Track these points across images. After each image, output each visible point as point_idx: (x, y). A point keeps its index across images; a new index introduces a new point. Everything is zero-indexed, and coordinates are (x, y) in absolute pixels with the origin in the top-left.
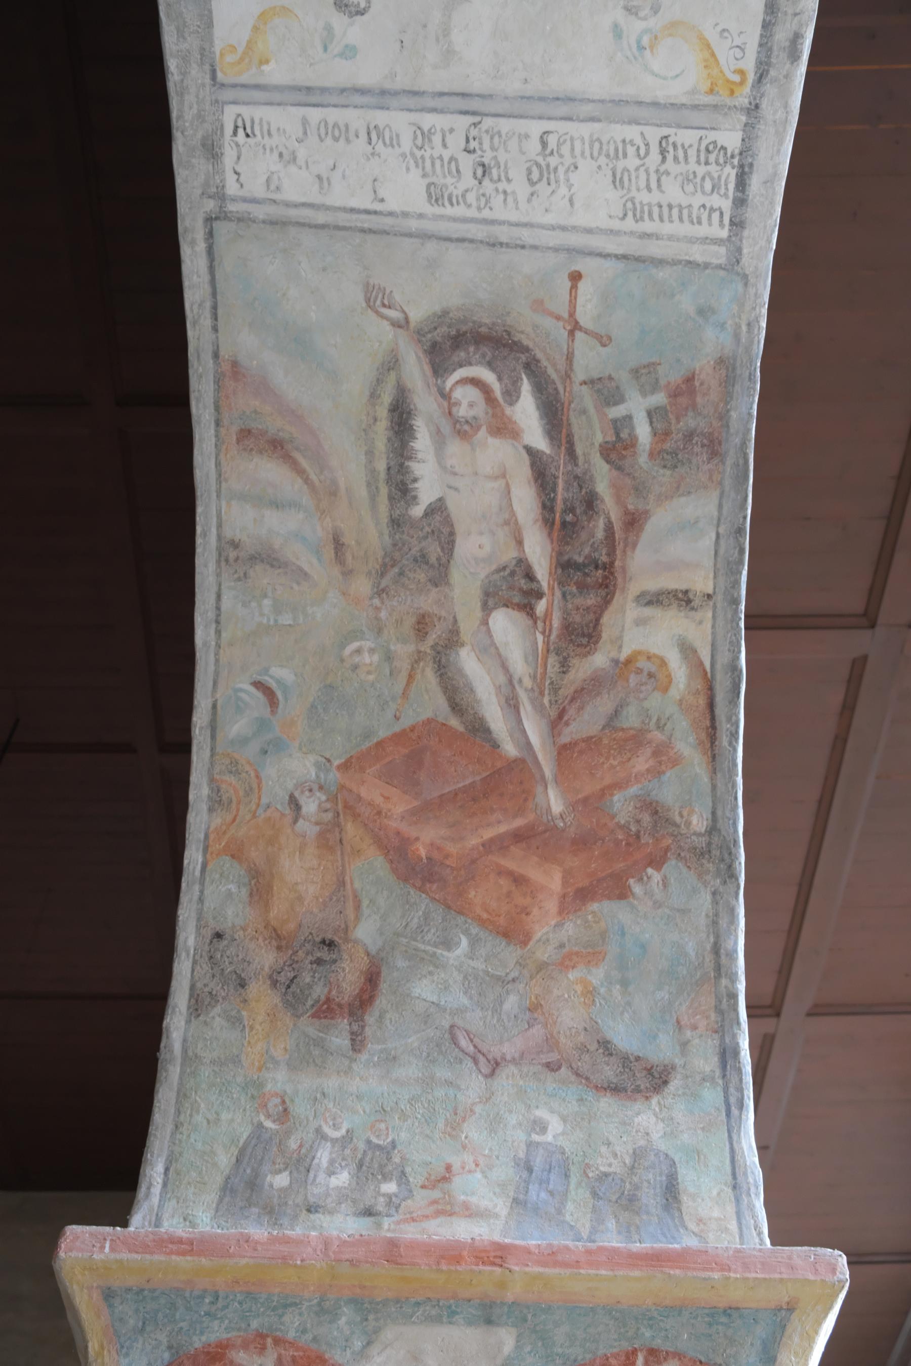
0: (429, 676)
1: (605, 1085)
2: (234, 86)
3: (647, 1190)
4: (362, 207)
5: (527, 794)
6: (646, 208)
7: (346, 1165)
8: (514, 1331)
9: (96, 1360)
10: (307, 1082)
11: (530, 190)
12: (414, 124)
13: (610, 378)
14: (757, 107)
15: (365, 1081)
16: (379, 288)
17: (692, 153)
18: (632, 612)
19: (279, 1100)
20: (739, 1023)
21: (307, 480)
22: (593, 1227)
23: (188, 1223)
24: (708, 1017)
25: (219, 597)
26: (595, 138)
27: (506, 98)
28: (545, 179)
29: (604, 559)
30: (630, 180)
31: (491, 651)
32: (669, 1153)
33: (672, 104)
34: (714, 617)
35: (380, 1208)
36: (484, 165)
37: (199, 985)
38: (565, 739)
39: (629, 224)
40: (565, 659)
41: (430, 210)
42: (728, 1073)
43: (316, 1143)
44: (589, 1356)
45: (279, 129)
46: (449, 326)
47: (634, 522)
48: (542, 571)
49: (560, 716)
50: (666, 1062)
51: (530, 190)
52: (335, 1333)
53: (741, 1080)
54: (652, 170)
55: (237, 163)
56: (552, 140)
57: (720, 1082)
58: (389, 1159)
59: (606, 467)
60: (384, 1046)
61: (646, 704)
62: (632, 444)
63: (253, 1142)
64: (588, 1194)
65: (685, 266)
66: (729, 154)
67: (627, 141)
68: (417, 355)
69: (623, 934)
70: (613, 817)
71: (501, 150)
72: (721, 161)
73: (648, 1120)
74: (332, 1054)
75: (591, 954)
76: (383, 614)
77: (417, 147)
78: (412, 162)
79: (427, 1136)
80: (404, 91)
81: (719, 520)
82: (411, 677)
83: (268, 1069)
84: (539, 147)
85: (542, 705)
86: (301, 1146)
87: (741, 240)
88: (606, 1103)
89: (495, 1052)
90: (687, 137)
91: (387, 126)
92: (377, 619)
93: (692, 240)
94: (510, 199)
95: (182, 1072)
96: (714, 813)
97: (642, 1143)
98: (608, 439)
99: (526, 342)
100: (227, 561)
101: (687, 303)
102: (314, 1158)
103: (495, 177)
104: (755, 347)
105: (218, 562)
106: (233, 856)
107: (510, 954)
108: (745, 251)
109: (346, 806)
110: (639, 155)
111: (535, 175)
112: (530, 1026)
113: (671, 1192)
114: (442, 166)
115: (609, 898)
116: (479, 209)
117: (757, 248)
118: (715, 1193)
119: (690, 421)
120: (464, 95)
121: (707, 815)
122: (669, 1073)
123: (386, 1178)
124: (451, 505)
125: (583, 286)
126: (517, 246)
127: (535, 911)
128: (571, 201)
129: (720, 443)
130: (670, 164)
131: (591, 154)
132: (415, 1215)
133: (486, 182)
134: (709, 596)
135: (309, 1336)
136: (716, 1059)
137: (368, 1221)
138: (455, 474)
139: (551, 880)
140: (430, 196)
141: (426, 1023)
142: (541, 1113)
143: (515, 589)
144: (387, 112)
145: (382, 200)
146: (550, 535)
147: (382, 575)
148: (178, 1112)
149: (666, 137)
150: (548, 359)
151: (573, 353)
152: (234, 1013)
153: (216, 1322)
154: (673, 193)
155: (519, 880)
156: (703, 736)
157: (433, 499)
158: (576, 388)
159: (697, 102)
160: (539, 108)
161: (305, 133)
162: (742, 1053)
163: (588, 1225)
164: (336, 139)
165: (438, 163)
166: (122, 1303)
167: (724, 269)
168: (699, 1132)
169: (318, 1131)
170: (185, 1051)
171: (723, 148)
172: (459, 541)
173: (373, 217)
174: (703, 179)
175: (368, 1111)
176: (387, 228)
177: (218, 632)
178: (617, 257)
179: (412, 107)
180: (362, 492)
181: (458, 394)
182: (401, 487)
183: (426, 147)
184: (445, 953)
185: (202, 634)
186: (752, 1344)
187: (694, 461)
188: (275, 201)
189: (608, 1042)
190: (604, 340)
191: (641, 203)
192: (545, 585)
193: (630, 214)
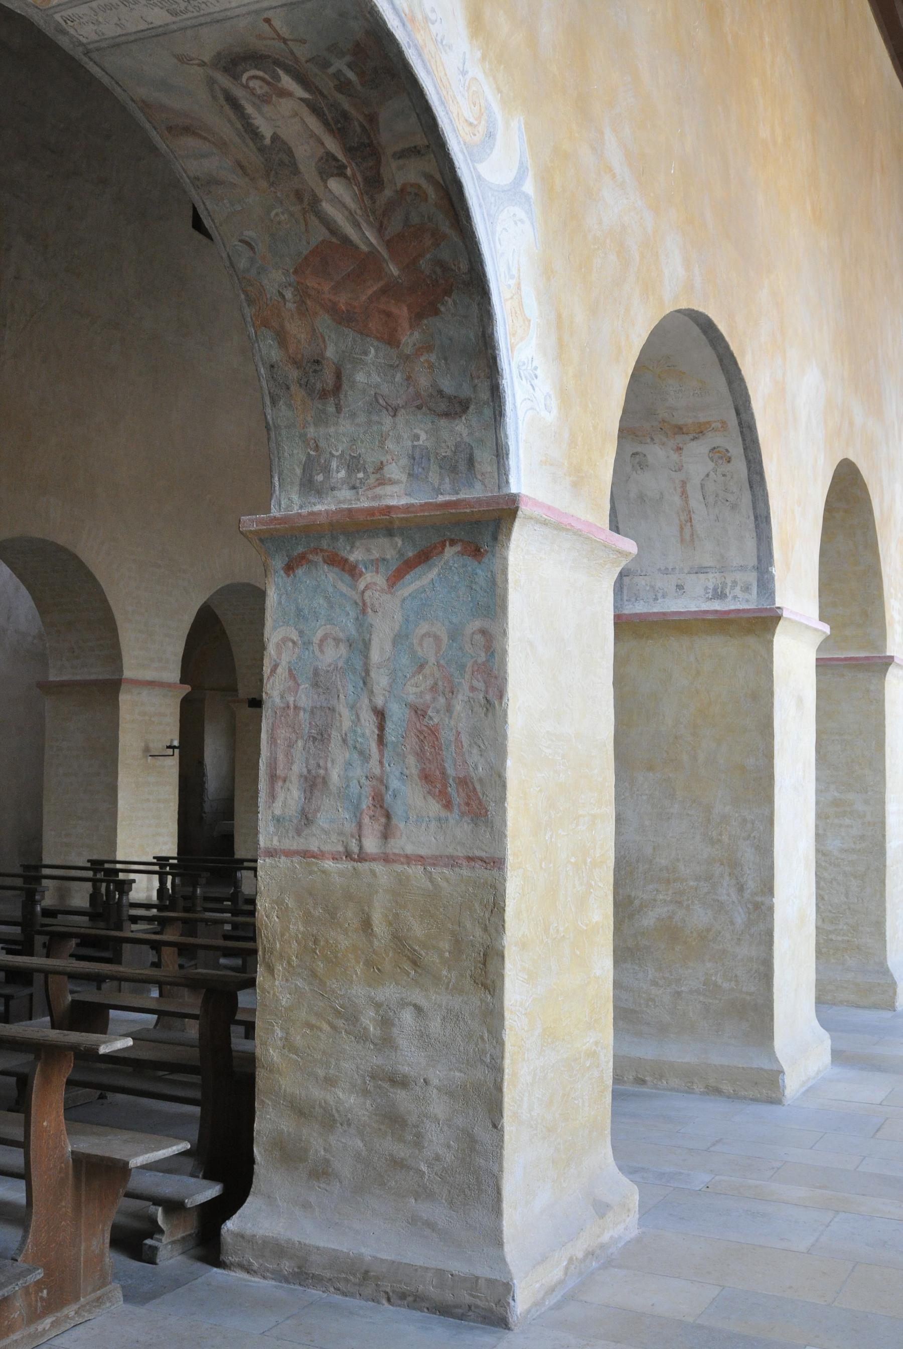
10: (322, 430)
15: (345, 426)
18: (394, 164)
21: (209, 141)
25: (204, 203)
29: (367, 141)
31: (336, 201)
35: (358, 485)
47: (372, 119)
48: (340, 156)
62: (349, 82)
82: (305, 221)
88: (443, 422)
96: (470, 261)
97: (459, 439)
123: (359, 471)
137: (354, 491)
142: (417, 431)
143: (331, 167)
146: (335, 137)
155: (389, 315)
157: (271, 134)
169: (331, 453)
170: (274, 423)
181: (251, 84)
182: (254, 133)
190: (304, 42)
192: (344, 161)
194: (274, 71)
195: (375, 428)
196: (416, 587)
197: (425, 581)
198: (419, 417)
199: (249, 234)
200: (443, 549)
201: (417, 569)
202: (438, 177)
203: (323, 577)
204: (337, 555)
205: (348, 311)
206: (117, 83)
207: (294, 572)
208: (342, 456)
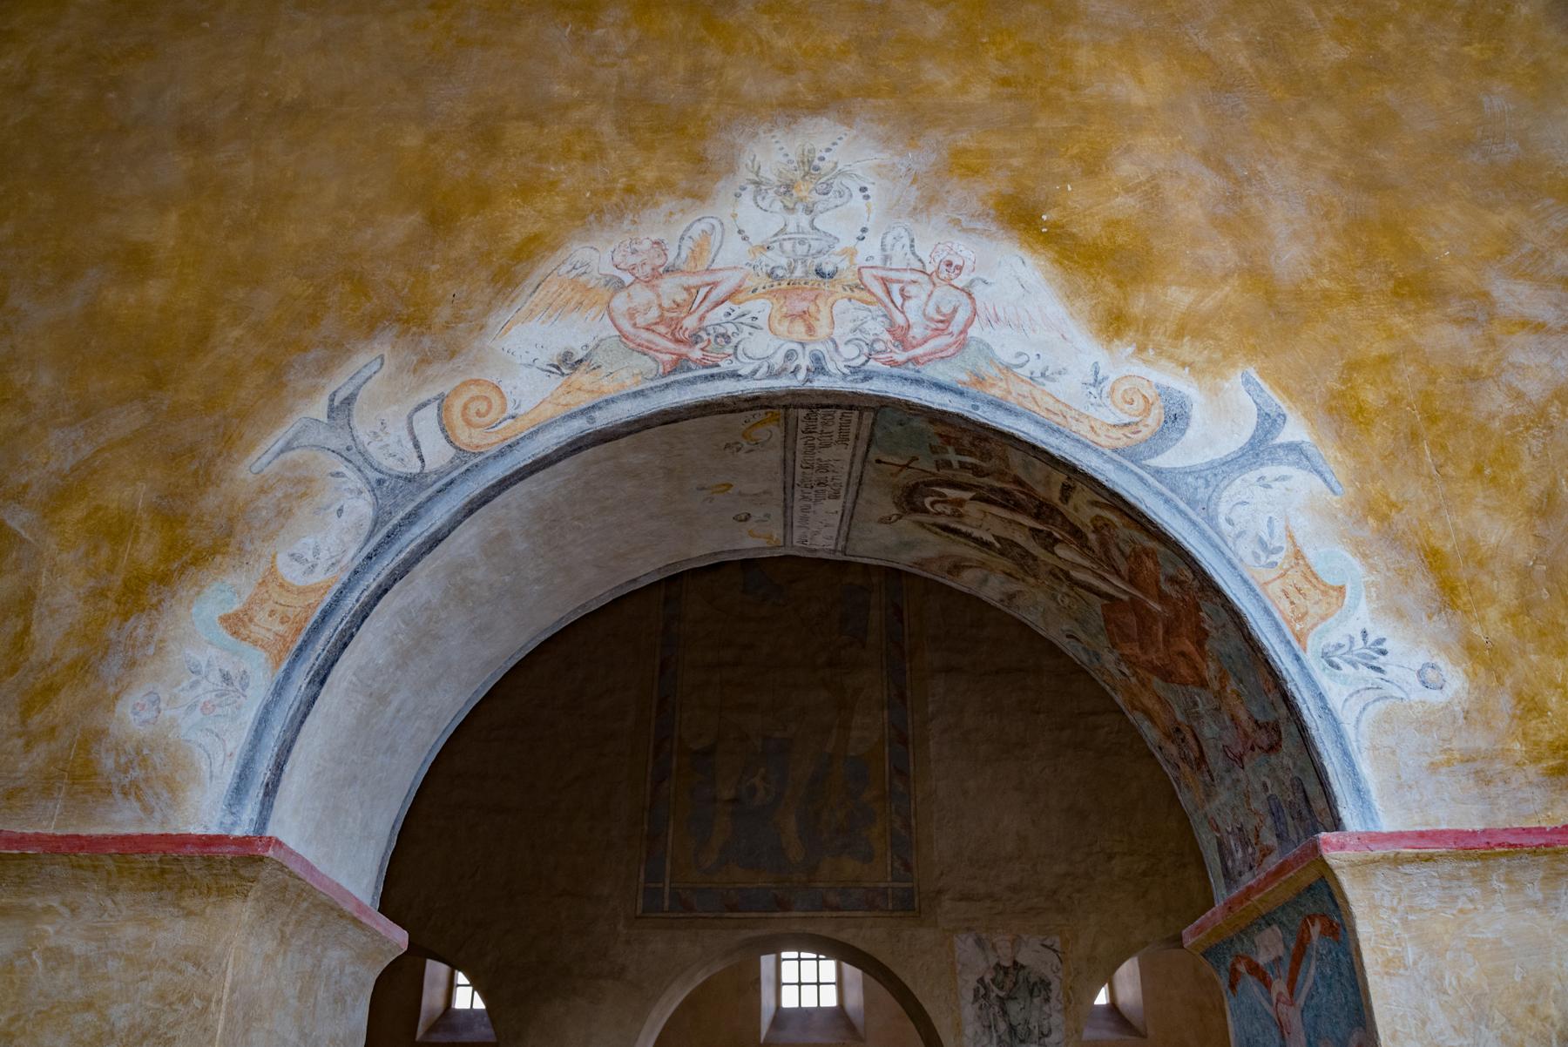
39: (851, 443)
47: (1018, 481)
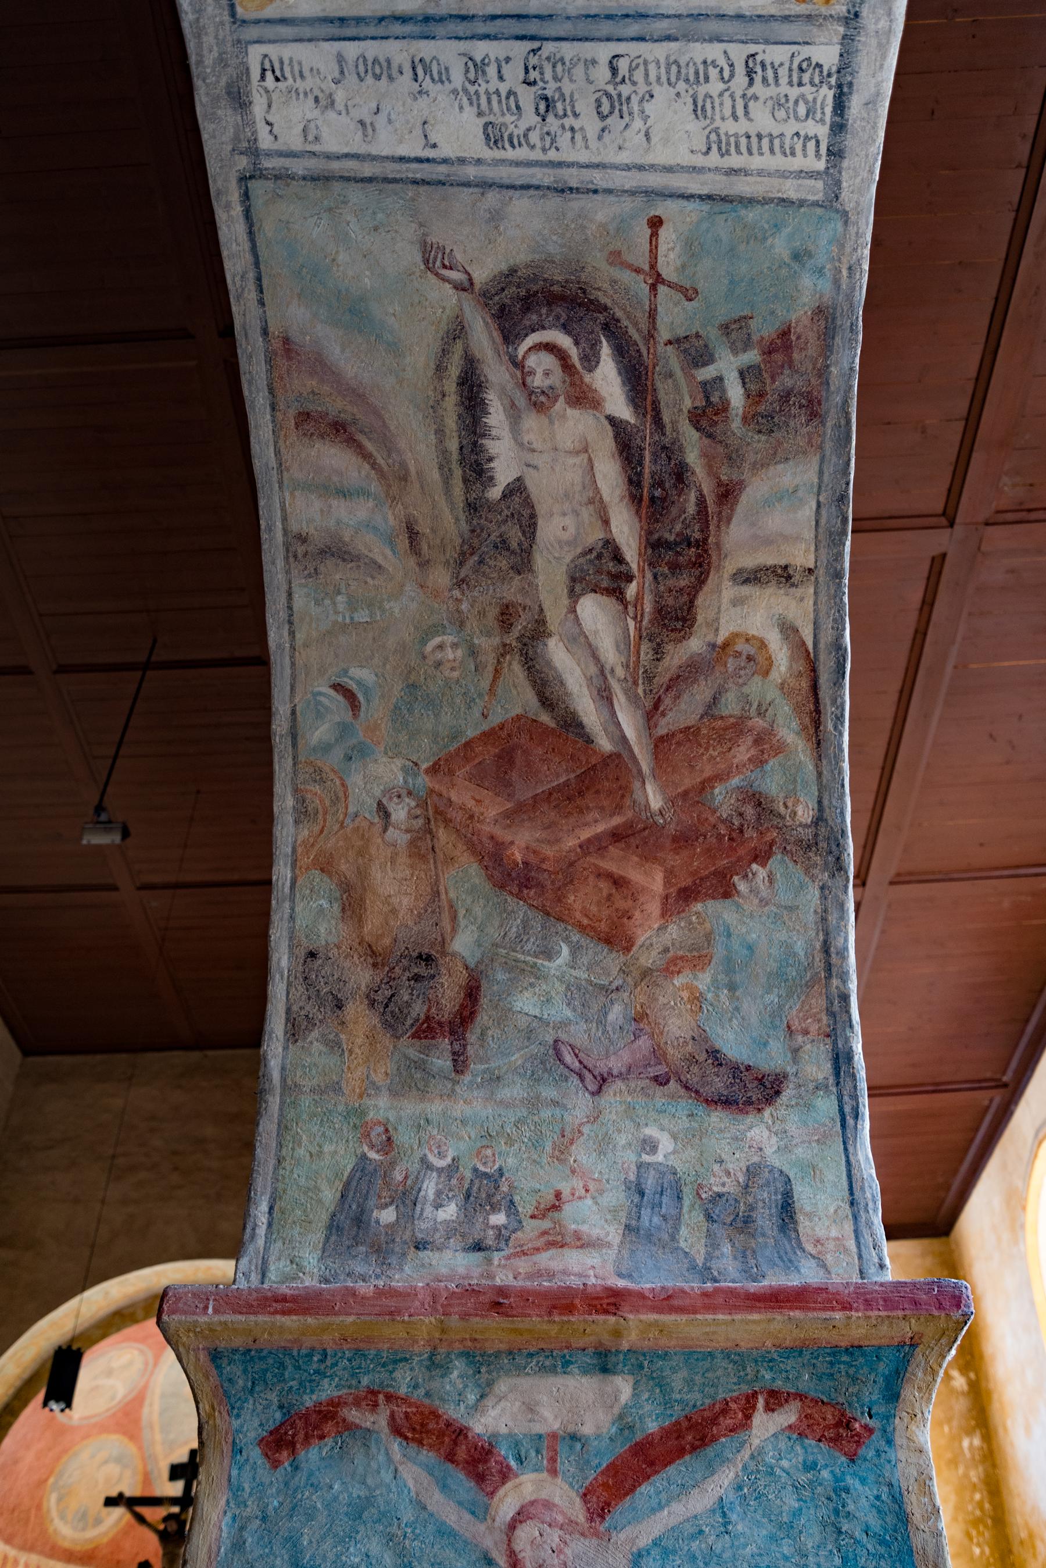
0: (516, 670)
1: (716, 1098)
2: (257, 22)
3: (762, 1211)
4: (413, 155)
5: (625, 790)
6: (732, 140)
7: (454, 1196)
8: (631, 1379)
9: (207, 1422)
10: (410, 1108)
11: (600, 125)
12: (464, 55)
13: (698, 336)
14: (857, 15)
15: (470, 1104)
16: (438, 247)
17: (783, 72)
18: (729, 591)
19: (381, 1129)
20: (851, 1026)
21: (374, 465)
22: (708, 1253)
23: (295, 1266)
24: (819, 1021)
25: (290, 595)
26: (671, 60)
27: (568, 18)
28: (617, 111)
29: (697, 535)
30: (713, 108)
31: (582, 642)
32: (784, 1169)
33: (759, 16)
34: (816, 593)
35: (490, 1242)
36: (546, 99)
37: (295, 1008)
38: (661, 731)
39: (714, 159)
40: (658, 644)
41: (488, 154)
42: (841, 1080)
43: (422, 1174)
44: (708, 1401)
45: (312, 69)
46: (518, 287)
47: (728, 494)
49: (656, 706)
50: (778, 1071)
51: (600, 125)
52: (448, 1387)
53: (855, 1087)
54: (738, 94)
55: (268, 112)
56: (623, 65)
57: (834, 1090)
58: (497, 1188)
59: (695, 435)
60: (486, 1066)
61: (746, 690)
62: (724, 407)
63: (358, 1175)
64: (701, 1218)
65: (777, 205)
66: (825, 73)
67: (709, 61)
68: (484, 321)
69: (729, 935)
70: (714, 812)
71: (566, 80)
72: (817, 80)
73: (762, 1136)
74: (434, 1077)
75: (697, 958)
76: (464, 606)
77: (470, 81)
78: (465, 99)
79: (534, 1161)
80: (451, 16)
81: (820, 487)
83: (369, 1095)
84: (608, 74)
85: (637, 695)
86: (406, 1177)
87: (840, 173)
88: (717, 1118)
89: (602, 1067)
90: (777, 54)
91: (434, 58)
92: (458, 611)
93: (783, 175)
94: (578, 137)
95: (282, 1103)
96: (820, 802)
97: (756, 1159)
98: (698, 404)
99: (604, 300)
100: (295, 557)
101: (780, 246)
102: (420, 1189)
103: (561, 113)
104: (857, 293)
105: (287, 558)
106: (322, 870)
107: (613, 961)
108: (844, 184)
109: (437, 812)
110: (723, 78)
111: (606, 108)
112: (636, 1037)
113: (787, 1211)
114: (500, 102)
115: (714, 898)
116: (544, 150)
117: (858, 180)
118: (832, 1210)
119: (787, 380)
120: (519, 17)
121: (813, 804)
122: (782, 1082)
123: (495, 1209)
124: (529, 483)
125: (665, 234)
126: (588, 191)
127: (637, 914)
128: (647, 135)
129: (819, 403)
130: (758, 88)
131: (668, 79)
132: (525, 1248)
133: (550, 118)
134: (810, 570)
135: (421, 1392)
136: (829, 1065)
137: (479, 1256)
138: (534, 451)
139: (652, 881)
140: (487, 137)
141: (529, 1038)
143: (602, 571)
144: (433, 42)
145: (434, 146)
146: (637, 512)
147: (461, 564)
148: (280, 1145)
149: (753, 55)
150: (628, 318)
151: (656, 310)
152: (331, 1037)
153: (326, 1380)
154: (763, 120)
155: (619, 882)
156: (807, 720)
157: (510, 480)
158: (660, 348)
159: (787, 13)
160: (606, 28)
161: (342, 72)
162: (856, 1058)
163: (703, 1251)
164: (378, 77)
165: (494, 98)
166: (229, 1364)
167: (822, 206)
168: (814, 1144)
169: (423, 1160)
170: (283, 1079)
171: (819, 66)
172: (540, 522)
173: (425, 165)
174: (796, 102)
175: (473, 1137)
176: (442, 178)
177: (292, 634)
178: (700, 197)
179: (461, 34)
180: (436, 475)
181: (532, 361)
183: (480, 81)
184: (546, 963)
185: (276, 636)
186: (874, 1382)
187: (792, 424)
188: (314, 154)
189: (717, 1051)
190: (689, 294)
191: (726, 134)
192: (634, 566)
193: (715, 147)
194: (595, 345)
195: (546, 1113)
196: (673, 1522)
197: (700, 1502)
198: (659, 1102)
199: (361, 675)
200: (748, 1417)
201: (671, 1470)
202: (807, 634)
203: (387, 1476)
204: (435, 1415)
205: (526, 863)
206: (259, 279)
207: (294, 1452)
208: (454, 1166)
